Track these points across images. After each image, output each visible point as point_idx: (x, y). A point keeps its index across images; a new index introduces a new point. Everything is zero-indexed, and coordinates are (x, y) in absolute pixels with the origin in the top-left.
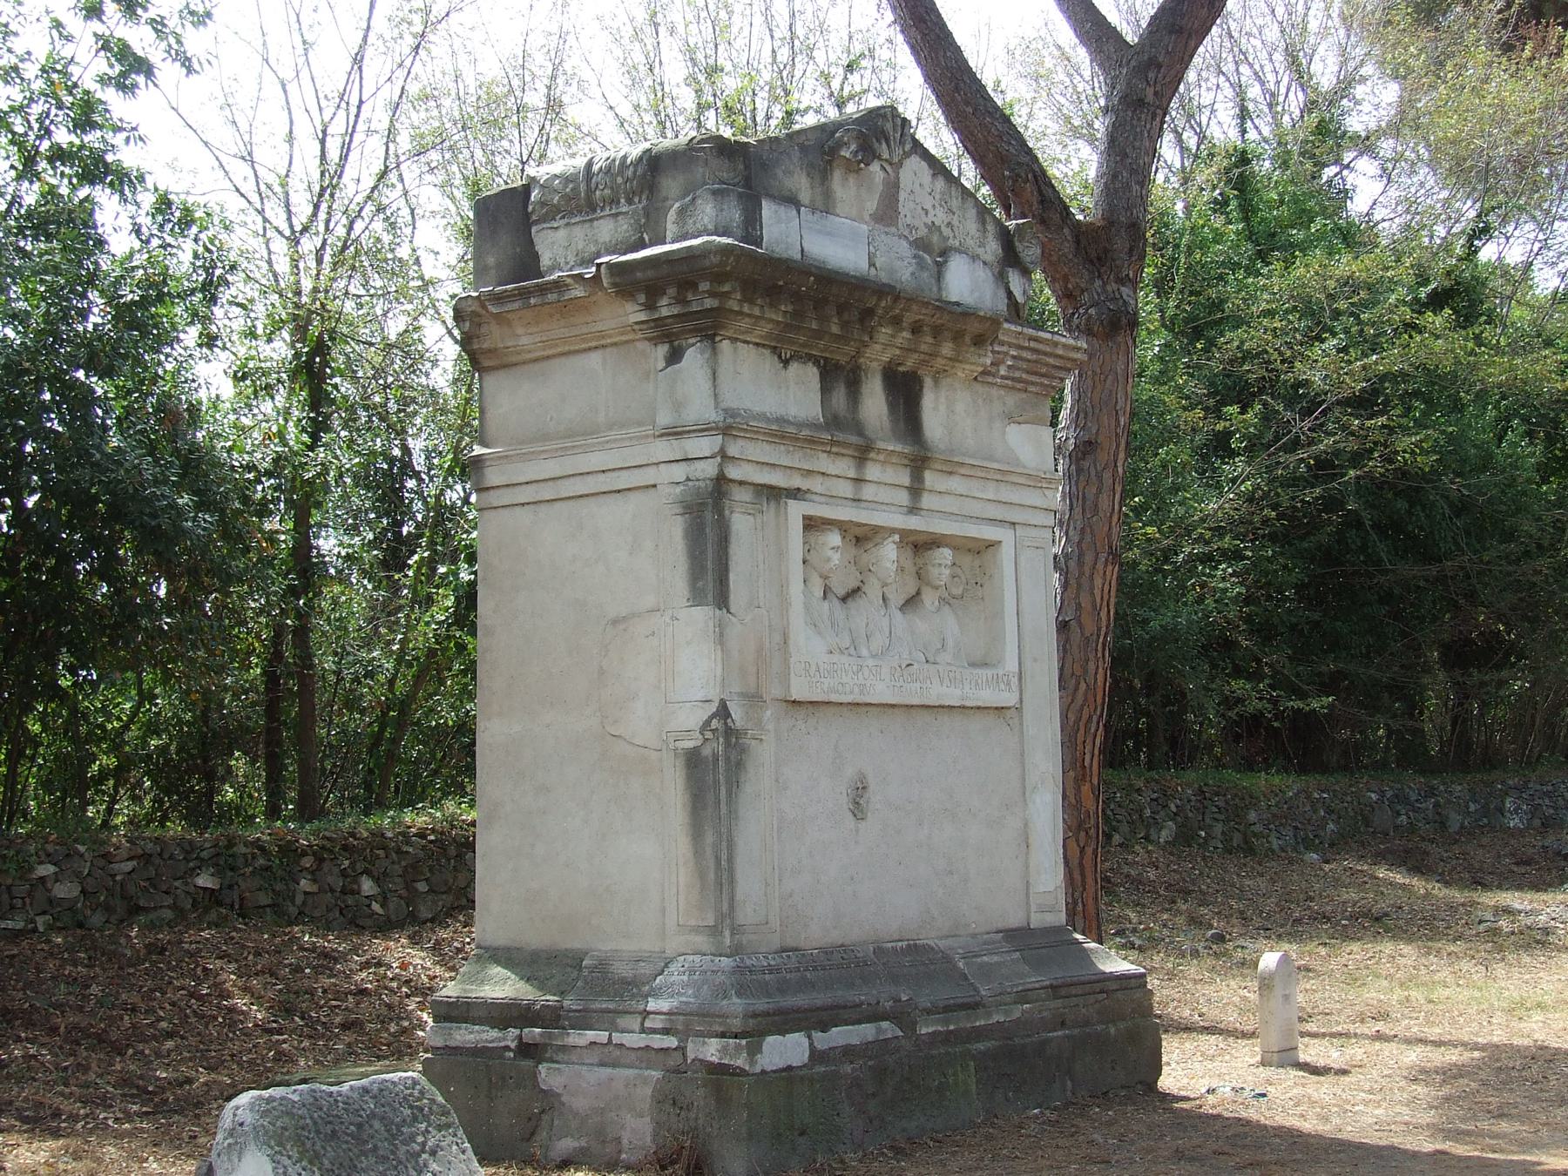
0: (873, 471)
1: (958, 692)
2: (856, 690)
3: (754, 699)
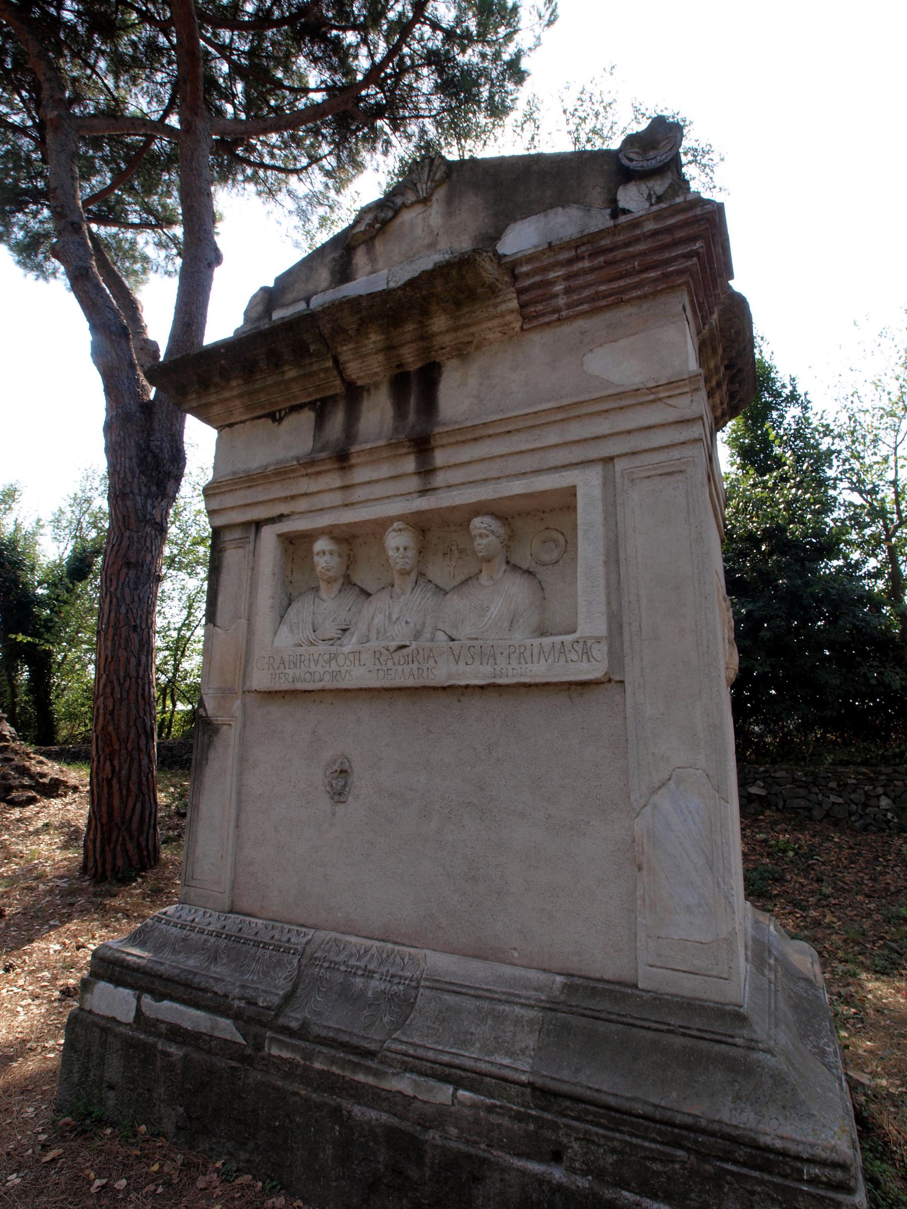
0: (360, 475)
1: (487, 669)
2: (327, 677)
3: (226, 693)
